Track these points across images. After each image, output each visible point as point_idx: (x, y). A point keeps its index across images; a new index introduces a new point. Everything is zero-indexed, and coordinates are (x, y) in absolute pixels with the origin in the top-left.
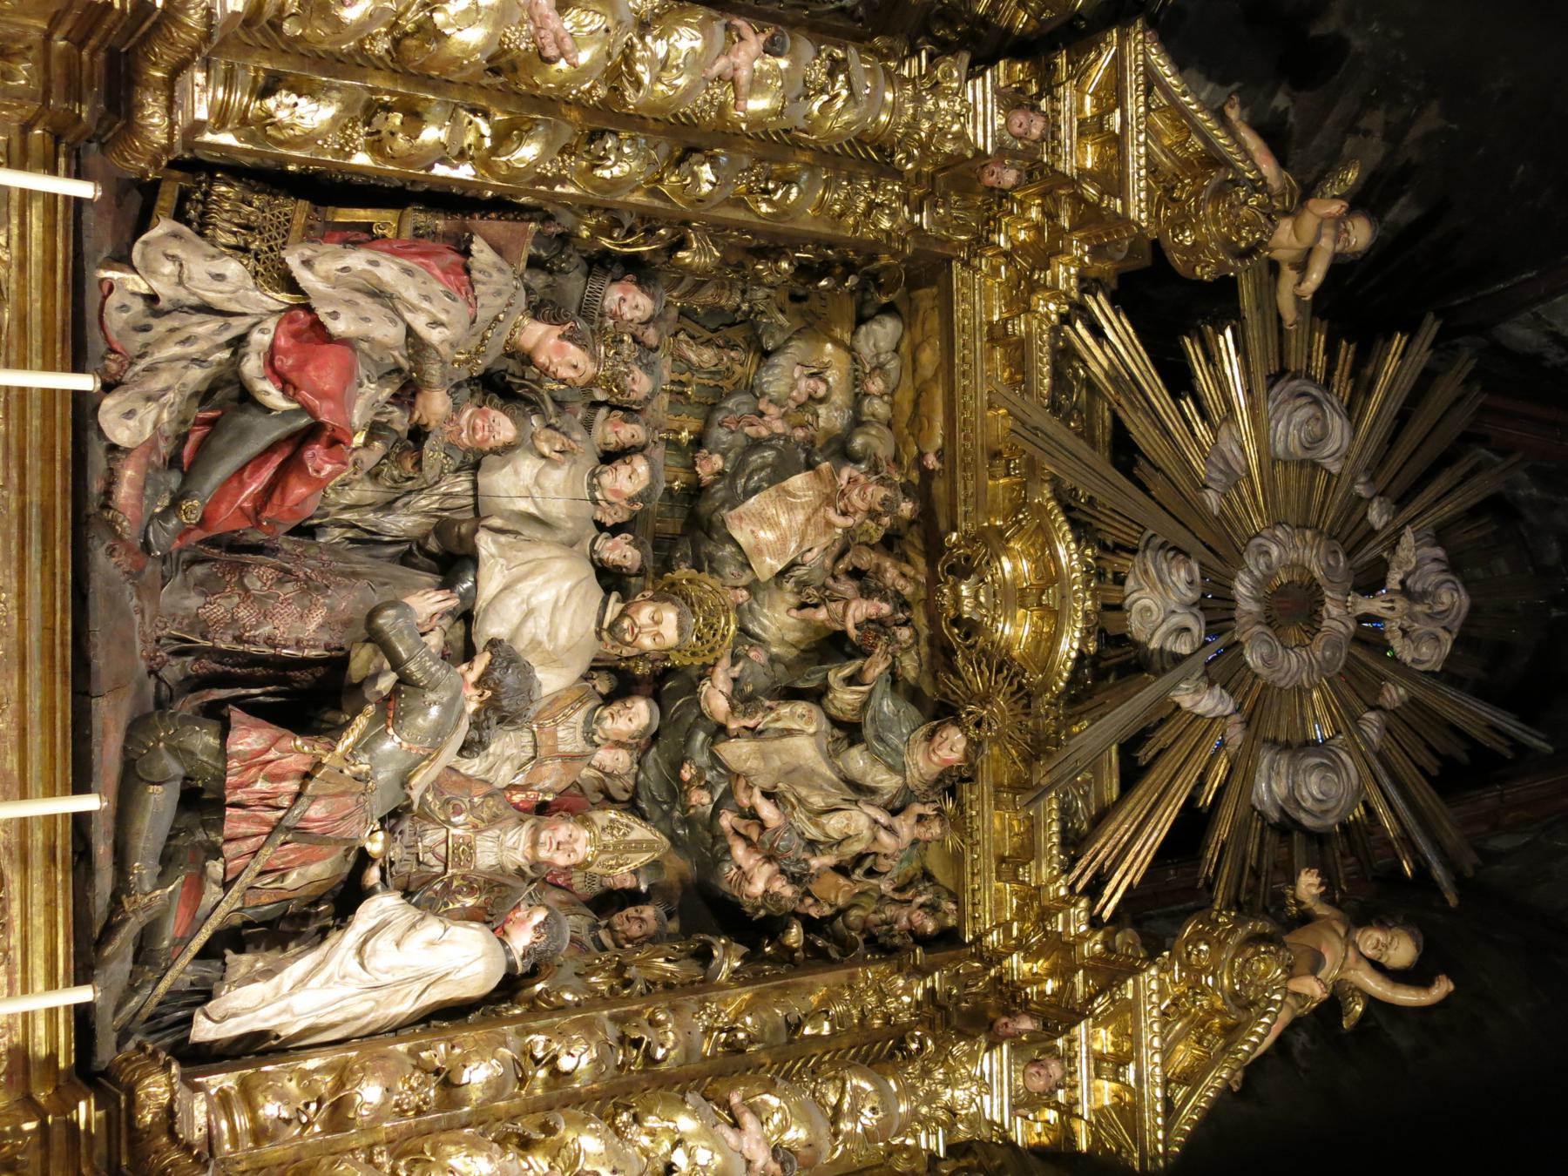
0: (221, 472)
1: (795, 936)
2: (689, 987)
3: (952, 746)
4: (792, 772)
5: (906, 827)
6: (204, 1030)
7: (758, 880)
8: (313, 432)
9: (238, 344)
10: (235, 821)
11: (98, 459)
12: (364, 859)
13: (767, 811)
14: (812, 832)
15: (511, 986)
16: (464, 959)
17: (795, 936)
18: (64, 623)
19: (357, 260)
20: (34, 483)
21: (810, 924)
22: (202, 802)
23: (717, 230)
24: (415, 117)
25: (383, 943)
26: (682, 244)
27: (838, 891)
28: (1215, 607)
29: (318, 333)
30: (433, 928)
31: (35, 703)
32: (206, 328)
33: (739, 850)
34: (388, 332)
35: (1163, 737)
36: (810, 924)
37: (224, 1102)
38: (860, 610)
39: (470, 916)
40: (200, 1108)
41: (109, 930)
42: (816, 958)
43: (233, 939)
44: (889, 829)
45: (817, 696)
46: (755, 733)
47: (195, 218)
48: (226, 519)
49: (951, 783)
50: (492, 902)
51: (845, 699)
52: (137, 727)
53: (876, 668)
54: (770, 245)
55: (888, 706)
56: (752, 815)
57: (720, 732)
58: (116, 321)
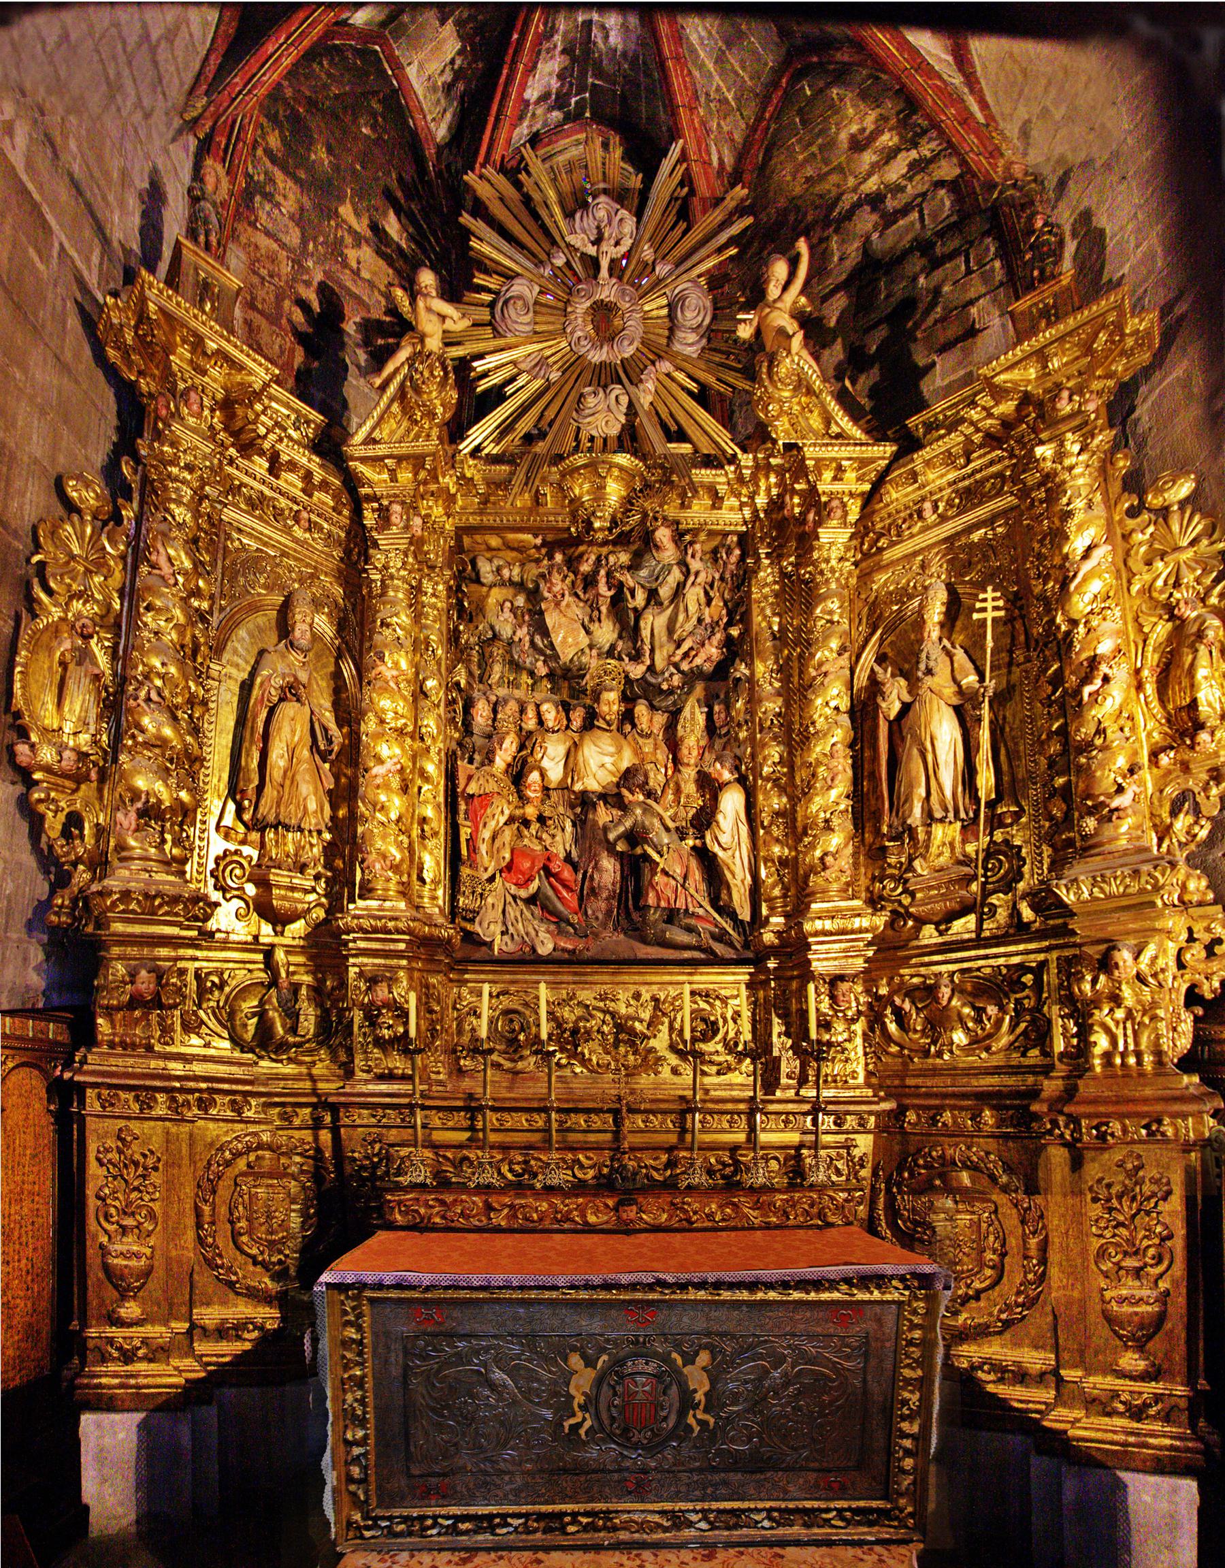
0: (559, 906)
1: (735, 632)
2: (751, 689)
3: (663, 535)
4: (671, 629)
5: (695, 565)
6: (745, 915)
7: (713, 651)
8: (546, 869)
9: (514, 897)
10: (680, 904)
11: (557, 954)
12: (694, 848)
13: (685, 647)
14: (694, 621)
15: (742, 780)
16: (732, 802)
17: (735, 632)
18: (611, 968)
19: (483, 848)
20: (565, 978)
21: (730, 624)
22: (671, 916)
23: (451, 670)
24: (424, 820)
25: (724, 839)
26: (458, 684)
27: (717, 602)
28: (606, 376)
29: (509, 867)
30: (720, 817)
31: (637, 978)
32: (512, 912)
33: (698, 661)
34: (508, 835)
35: (664, 415)
36: (730, 624)
37: (772, 909)
38: (603, 588)
39: (715, 799)
40: (773, 920)
41: (713, 952)
42: (746, 619)
43: (714, 901)
44: (697, 574)
45: (638, 614)
46: (652, 650)
47: (472, 915)
48: (574, 903)
49: (679, 536)
50: (710, 787)
51: (640, 598)
52: (644, 941)
53: (628, 579)
54: (453, 638)
55: (644, 573)
56: (686, 655)
57: (651, 669)
58: (511, 947)
